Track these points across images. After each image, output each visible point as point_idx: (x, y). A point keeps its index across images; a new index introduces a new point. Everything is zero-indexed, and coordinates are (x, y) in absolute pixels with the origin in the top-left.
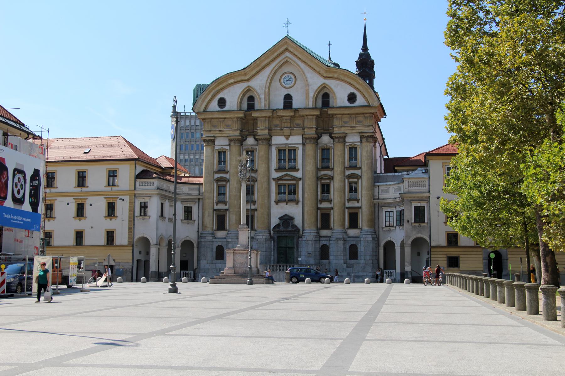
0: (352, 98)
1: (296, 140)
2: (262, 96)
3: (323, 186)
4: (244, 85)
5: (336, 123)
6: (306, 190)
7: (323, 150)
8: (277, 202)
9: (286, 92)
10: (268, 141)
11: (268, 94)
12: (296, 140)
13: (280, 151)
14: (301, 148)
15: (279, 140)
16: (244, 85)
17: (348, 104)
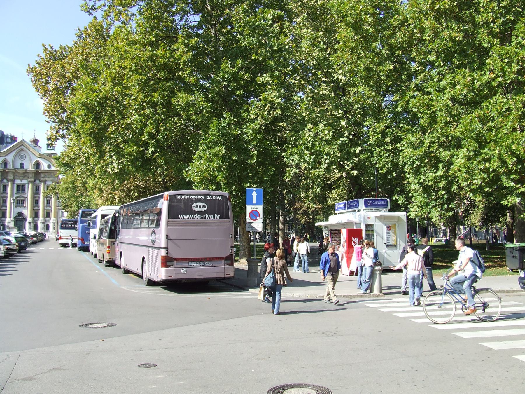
0: (49, 166)
1: (25, 182)
2: (11, 163)
3: (36, 200)
4: (3, 158)
5: (42, 175)
6: (29, 203)
7: (36, 186)
8: (16, 207)
9: (21, 162)
10: (13, 182)
11: (14, 162)
12: (25, 182)
13: (18, 186)
14: (27, 185)
15: (18, 181)
16: (3, 158)
17: (48, 169)
